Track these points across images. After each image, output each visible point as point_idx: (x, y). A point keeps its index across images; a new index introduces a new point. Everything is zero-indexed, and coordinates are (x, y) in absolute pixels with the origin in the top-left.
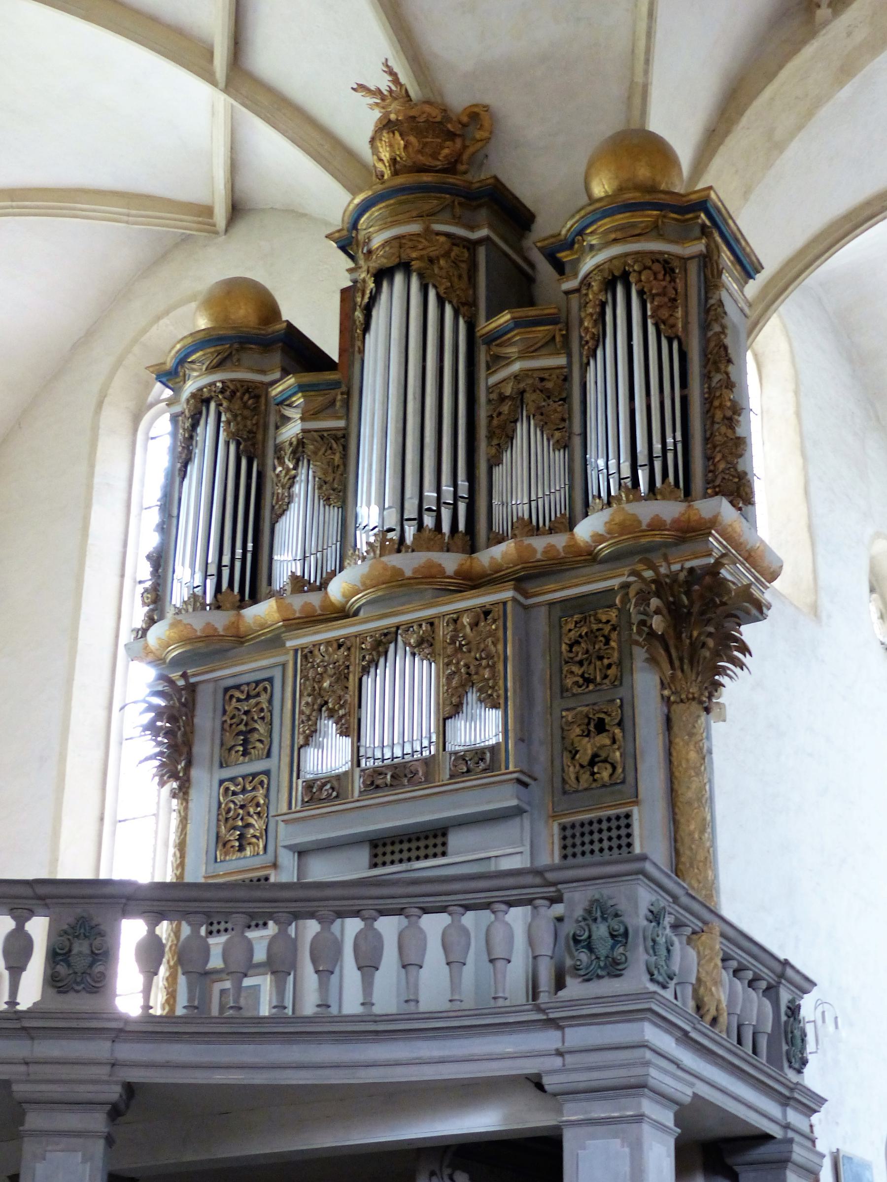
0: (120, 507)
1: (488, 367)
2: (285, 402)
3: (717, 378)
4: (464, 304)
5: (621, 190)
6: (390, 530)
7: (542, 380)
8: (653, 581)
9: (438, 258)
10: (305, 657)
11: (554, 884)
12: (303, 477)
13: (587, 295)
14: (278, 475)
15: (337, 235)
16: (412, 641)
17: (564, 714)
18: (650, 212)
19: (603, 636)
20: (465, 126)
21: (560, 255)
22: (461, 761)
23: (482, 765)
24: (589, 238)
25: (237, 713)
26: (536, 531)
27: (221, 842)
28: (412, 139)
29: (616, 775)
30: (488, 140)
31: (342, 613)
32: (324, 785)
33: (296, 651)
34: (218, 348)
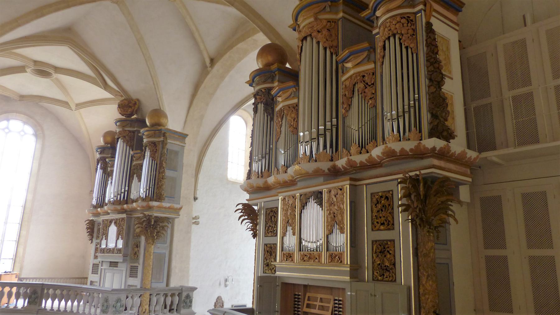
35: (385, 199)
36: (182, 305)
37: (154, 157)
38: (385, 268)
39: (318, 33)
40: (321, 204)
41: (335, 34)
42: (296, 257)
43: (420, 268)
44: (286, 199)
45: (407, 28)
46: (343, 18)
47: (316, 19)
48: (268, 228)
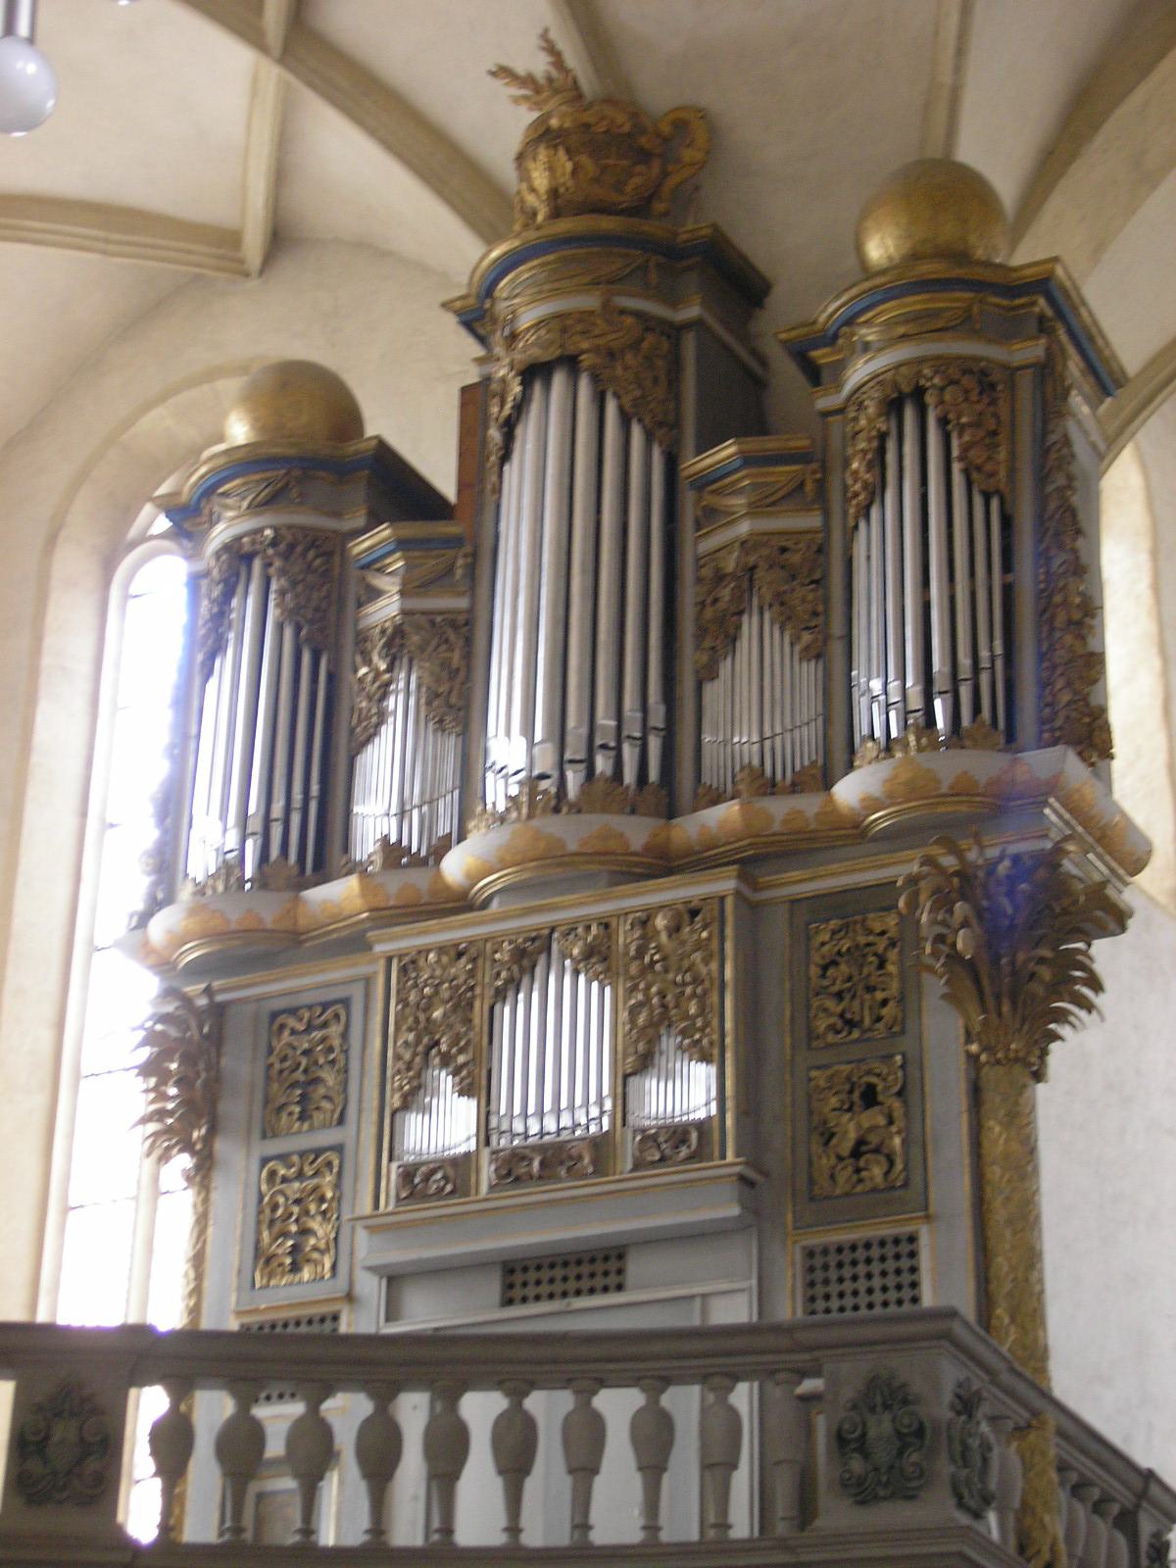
0: (80, 704)
1: (698, 526)
2: (374, 565)
3: (1059, 560)
4: (660, 424)
5: (914, 257)
6: (543, 777)
7: (784, 550)
8: (957, 874)
9: (622, 351)
10: (403, 970)
11: (810, 1349)
12: (401, 685)
13: (856, 419)
14: (361, 680)
15: (458, 304)
16: (576, 951)
17: (814, 1074)
18: (958, 294)
19: (875, 954)
20: (666, 140)
21: (814, 354)
22: (650, 1144)
23: (684, 1152)
24: (864, 331)
25: (290, 1052)
26: (769, 787)
27: (264, 1259)
28: (584, 159)
29: (893, 1175)
30: (703, 164)
31: (461, 902)
32: (433, 1172)
33: (389, 960)
34: (269, 474)
37: (989, 467)
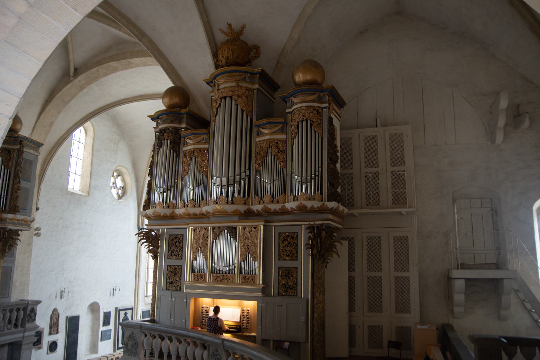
35: (291, 238)
36: (27, 320)
37: (8, 165)
38: (289, 287)
39: (238, 97)
40: (235, 237)
41: (251, 101)
42: (209, 277)
43: (315, 286)
44: (197, 229)
45: (317, 118)
46: (258, 89)
47: (238, 86)
48: (172, 252)
